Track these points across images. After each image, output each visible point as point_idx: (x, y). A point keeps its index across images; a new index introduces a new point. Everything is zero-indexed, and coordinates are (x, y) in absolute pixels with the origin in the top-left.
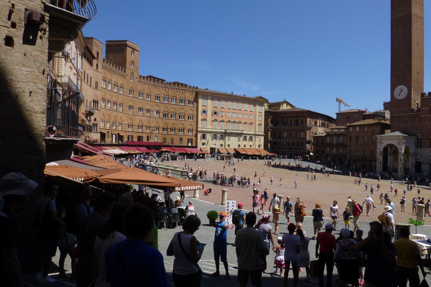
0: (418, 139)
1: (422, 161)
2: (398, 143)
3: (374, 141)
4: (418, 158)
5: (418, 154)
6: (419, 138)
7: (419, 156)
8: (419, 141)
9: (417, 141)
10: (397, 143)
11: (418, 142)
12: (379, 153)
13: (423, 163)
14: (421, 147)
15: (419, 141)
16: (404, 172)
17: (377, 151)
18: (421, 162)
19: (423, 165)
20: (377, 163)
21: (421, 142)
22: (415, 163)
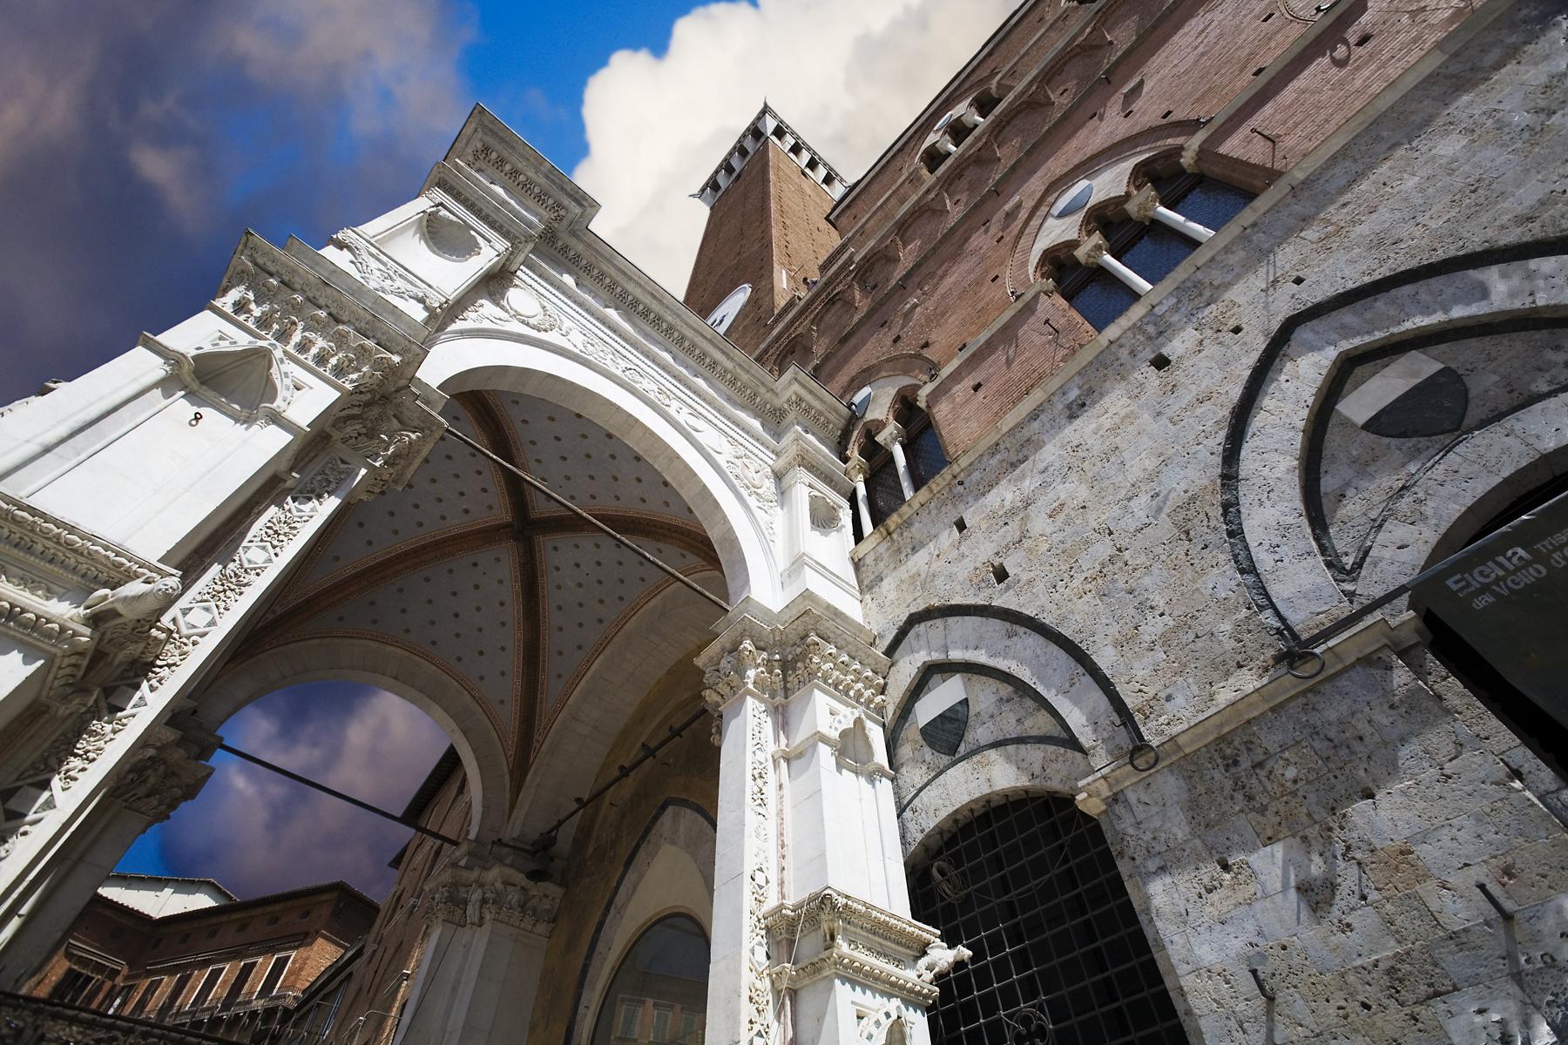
18: (1054, 770)
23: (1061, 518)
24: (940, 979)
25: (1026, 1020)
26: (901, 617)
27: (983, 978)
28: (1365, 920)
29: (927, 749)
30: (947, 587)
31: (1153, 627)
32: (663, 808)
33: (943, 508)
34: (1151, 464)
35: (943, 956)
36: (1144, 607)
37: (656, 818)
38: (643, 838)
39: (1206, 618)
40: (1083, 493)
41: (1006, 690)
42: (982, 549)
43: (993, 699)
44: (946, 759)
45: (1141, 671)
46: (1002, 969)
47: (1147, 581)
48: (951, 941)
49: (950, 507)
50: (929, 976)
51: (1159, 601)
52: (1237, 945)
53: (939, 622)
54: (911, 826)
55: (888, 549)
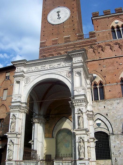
0: (95, 85)
1: (110, 129)
3: (5, 100)
4: (99, 125)
6: (97, 81)
7: (102, 118)
8: (98, 86)
9: (93, 87)
10: (65, 74)
11: (96, 89)
13: (113, 134)
14: (103, 97)
15: (98, 86)
18: (107, 132)
19: (112, 138)
20: (9, 136)
21: (102, 88)
23: (113, 113)
27: (98, 142)
28: (120, 145)
31: (116, 126)
32: (63, 117)
34: (121, 114)
35: (96, 140)
36: (116, 125)
37: (62, 118)
38: (60, 119)
39: (120, 128)
40: (116, 112)
42: (106, 111)
43: (103, 124)
44: (98, 127)
45: (115, 129)
46: (99, 142)
47: (117, 123)
51: (117, 125)
52: (114, 145)
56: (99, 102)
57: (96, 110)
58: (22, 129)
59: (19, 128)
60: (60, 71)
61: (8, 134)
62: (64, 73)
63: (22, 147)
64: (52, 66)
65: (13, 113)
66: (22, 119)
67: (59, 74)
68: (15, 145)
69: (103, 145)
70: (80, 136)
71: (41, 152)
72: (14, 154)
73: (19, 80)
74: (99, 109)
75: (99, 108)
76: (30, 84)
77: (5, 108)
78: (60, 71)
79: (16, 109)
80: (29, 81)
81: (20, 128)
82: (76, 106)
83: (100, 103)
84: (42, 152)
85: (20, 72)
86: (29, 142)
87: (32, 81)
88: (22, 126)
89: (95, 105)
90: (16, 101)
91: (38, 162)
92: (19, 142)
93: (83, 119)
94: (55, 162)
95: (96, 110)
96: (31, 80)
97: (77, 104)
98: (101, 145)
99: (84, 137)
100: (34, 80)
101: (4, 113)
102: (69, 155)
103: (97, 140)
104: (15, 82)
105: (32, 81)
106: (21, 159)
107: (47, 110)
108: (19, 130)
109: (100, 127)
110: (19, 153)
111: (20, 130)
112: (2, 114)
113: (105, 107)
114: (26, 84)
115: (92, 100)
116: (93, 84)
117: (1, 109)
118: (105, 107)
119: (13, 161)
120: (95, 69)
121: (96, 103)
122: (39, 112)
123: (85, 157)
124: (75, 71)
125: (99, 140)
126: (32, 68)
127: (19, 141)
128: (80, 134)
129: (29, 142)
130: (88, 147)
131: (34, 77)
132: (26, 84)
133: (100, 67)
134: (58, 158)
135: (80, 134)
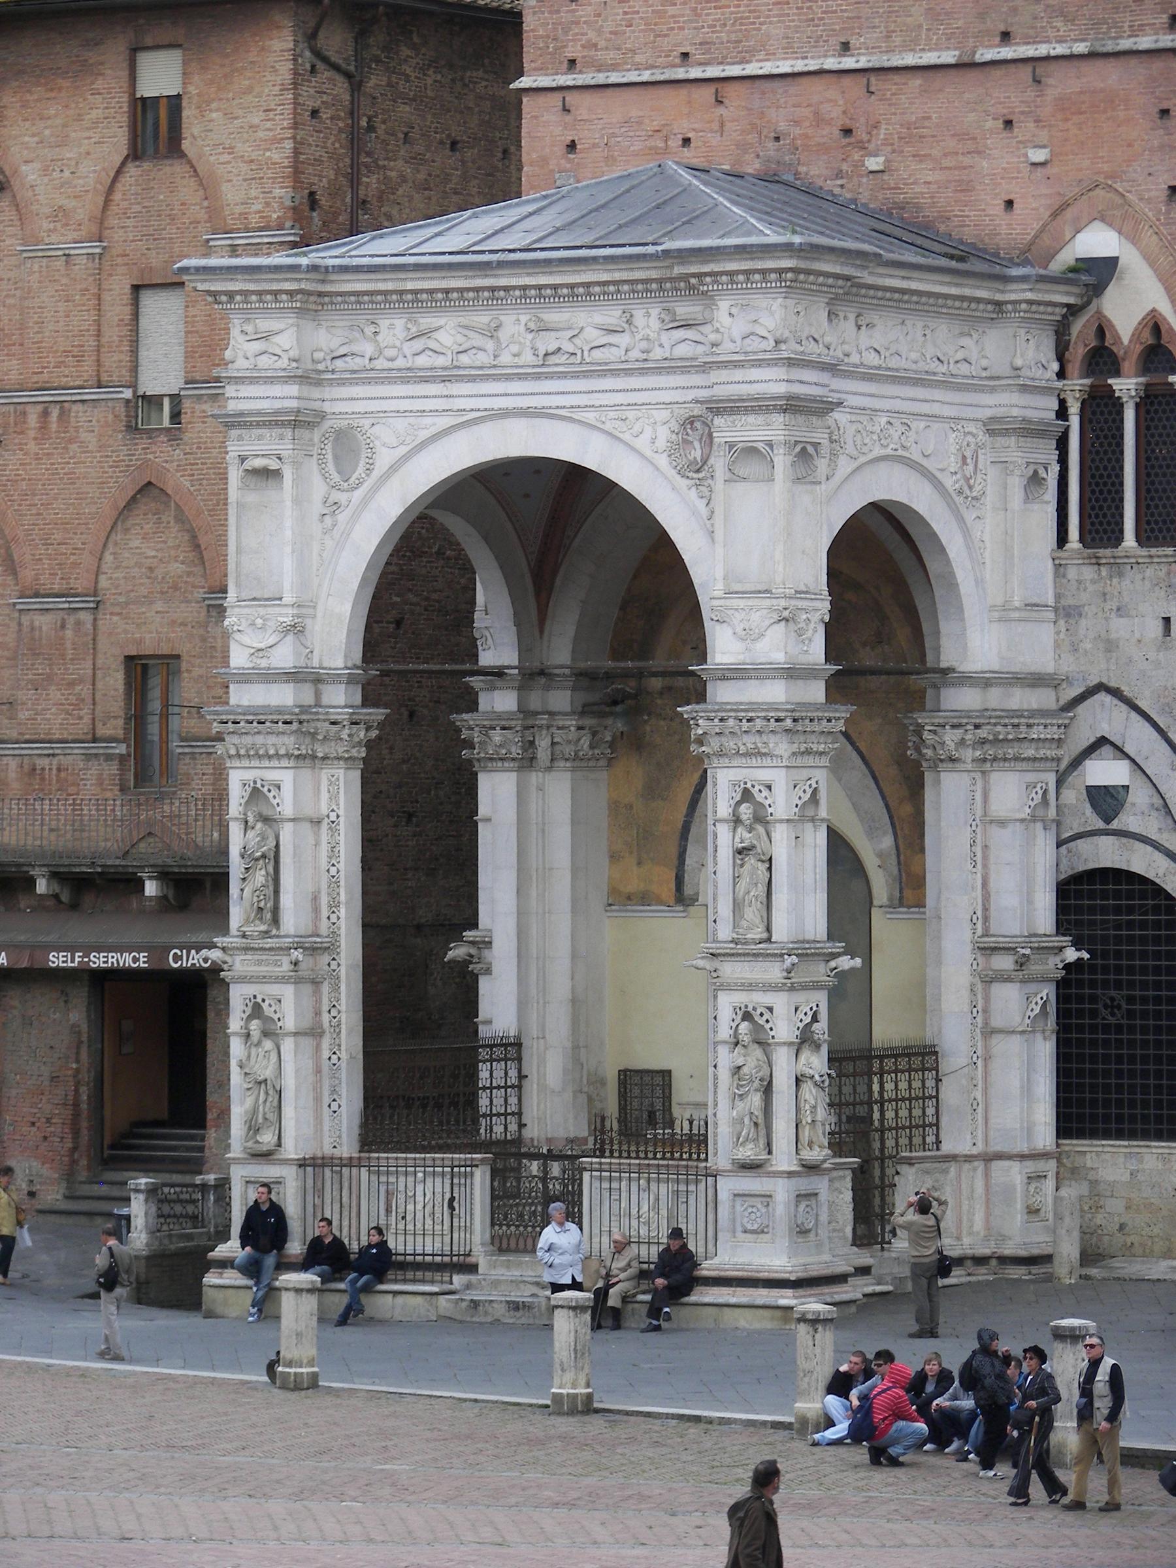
2: (681, 444)
5: (1101, 687)
8: (1126, 386)
9: (1077, 386)
10: (664, 435)
12: (283, 696)
15: (1126, 386)
16: (837, 1146)
17: (239, 658)
20: (239, 965)
22: (1044, 916)
24: (1068, 967)
25: (1112, 999)
26: (1091, 677)
27: (1092, 968)
29: (1088, 805)
30: (1139, 683)
33: (1157, 588)
35: (1071, 955)
41: (1158, 801)
43: (1147, 800)
44: (1101, 825)
48: (1077, 944)
49: (1163, 593)
50: (1061, 966)
53: (1124, 707)
54: (1064, 861)
55: (1093, 582)
56: (1117, 569)
57: (1088, 646)
58: (334, 906)
59: (315, 899)
60: (619, 398)
61: (224, 949)
62: (648, 433)
63: (344, 1055)
64: (548, 342)
65: (250, 775)
66: (333, 817)
67: (608, 426)
68: (288, 1045)
69: (1130, 1000)
70: (740, 998)
71: (569, 1045)
72: (288, 1111)
73: (273, 465)
74: (1110, 646)
75: (1120, 627)
76: (375, 489)
77: (174, 536)
78: (619, 398)
79: (272, 743)
80: (360, 469)
81: (324, 900)
82: (725, 761)
83: (1126, 582)
84: (576, 1048)
85: (271, 380)
86: (451, 954)
87: (394, 468)
88: (334, 882)
89: (1084, 597)
90: (264, 663)
91: (472, 1174)
92: (318, 1013)
93: (770, 869)
94: (586, 1176)
95: (1088, 646)
96: (385, 459)
97: (730, 744)
98: (1119, 1007)
99: (770, 1009)
100: (406, 458)
101: (175, 588)
102: (691, 1123)
103: (1086, 956)
104: (234, 476)
105: (394, 468)
106: (348, 1148)
107: (623, 608)
108: (316, 910)
109: (1115, 825)
110: (326, 1100)
111: (325, 912)
112: (159, 606)
113: (1167, 620)
114: (342, 497)
115: (1062, 538)
116: (1078, 353)
117: (136, 543)
118: (1167, 620)
119: (286, 1162)
120: (1106, 167)
121: (1088, 573)
122: (524, 650)
123: (770, 1153)
124: (731, 436)
125: (1105, 955)
126: (384, 323)
127: (319, 1001)
128: (750, 987)
129: (451, 954)
130: (798, 1081)
131: (400, 424)
132: (336, 496)
133: (1162, 147)
134: (625, 1147)
135: (750, 987)
